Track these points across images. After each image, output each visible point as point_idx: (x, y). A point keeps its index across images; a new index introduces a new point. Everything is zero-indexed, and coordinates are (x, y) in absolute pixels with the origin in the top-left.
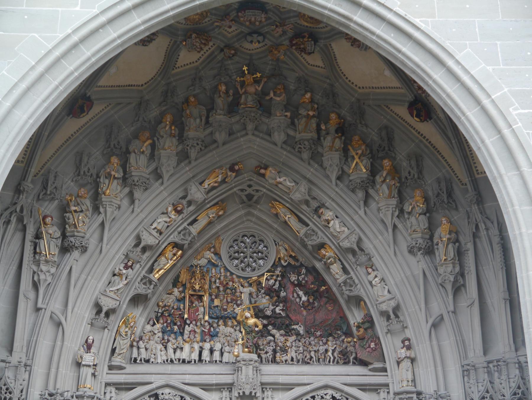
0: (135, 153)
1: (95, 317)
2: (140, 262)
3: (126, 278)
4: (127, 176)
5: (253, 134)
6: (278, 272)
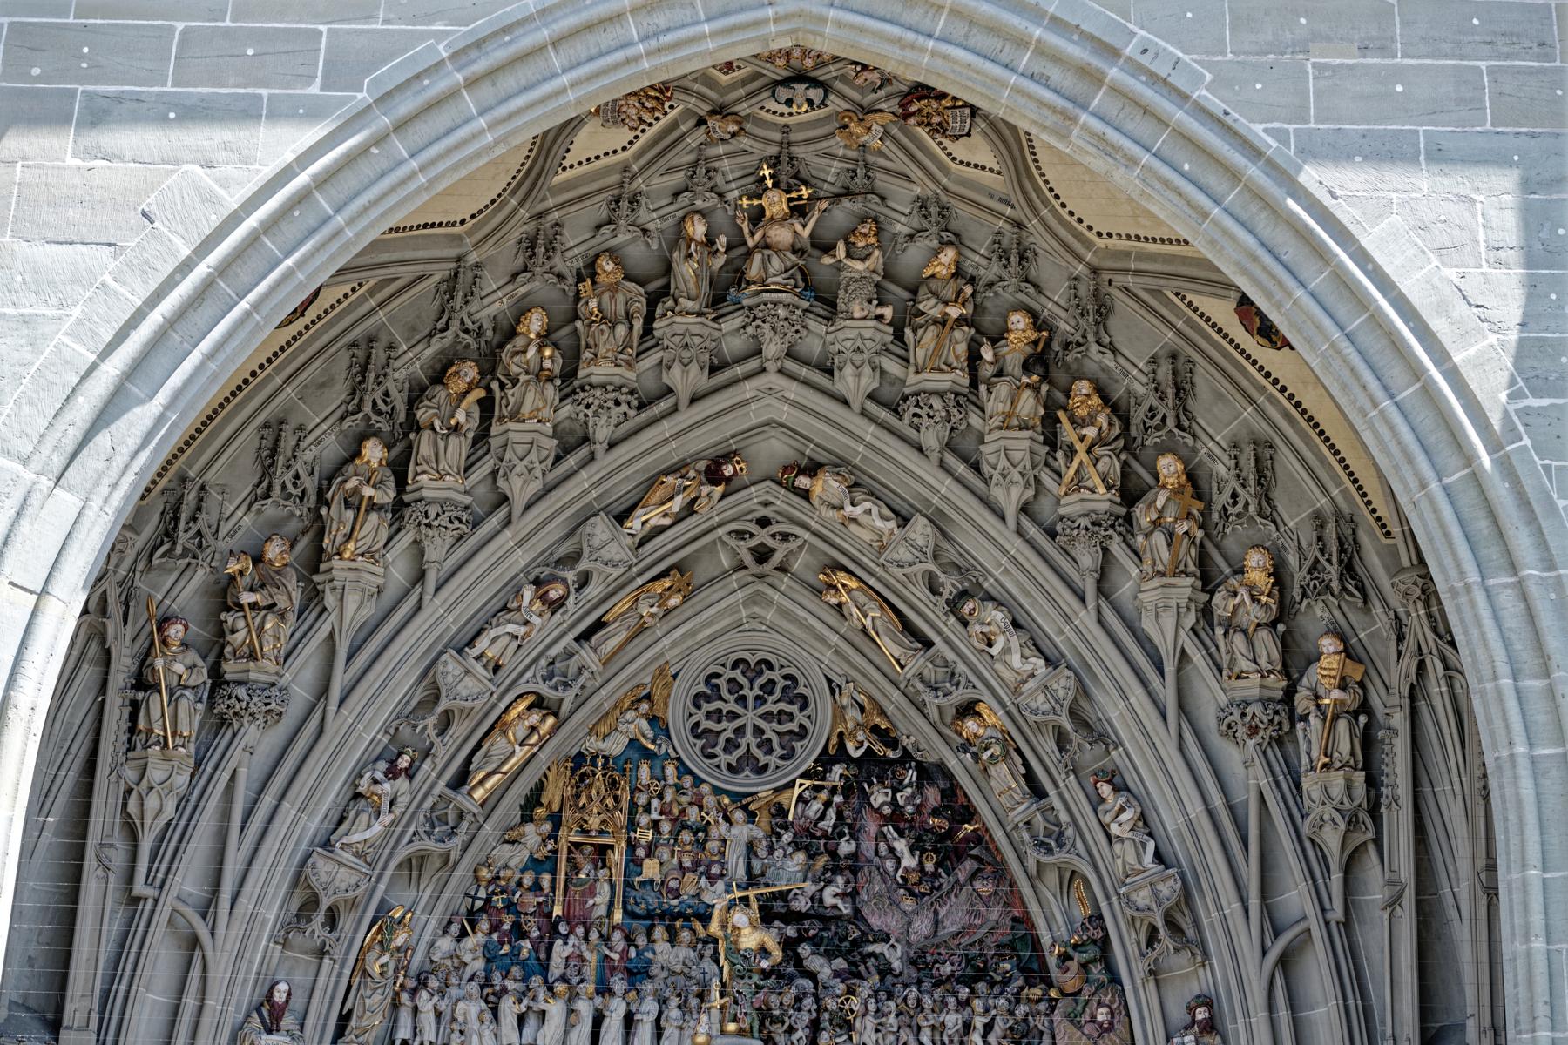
3: (392, 803)
4: (407, 498)
5: (781, 371)
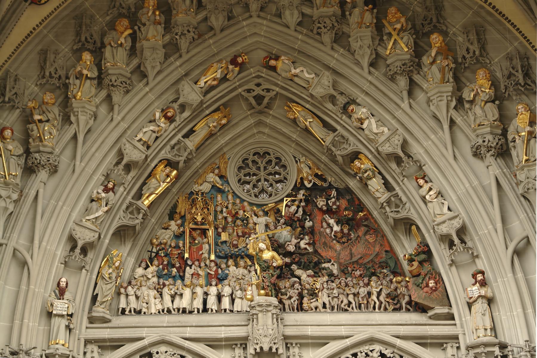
0: (112, 46)
1: (69, 254)
2: (124, 184)
6: (301, 195)
